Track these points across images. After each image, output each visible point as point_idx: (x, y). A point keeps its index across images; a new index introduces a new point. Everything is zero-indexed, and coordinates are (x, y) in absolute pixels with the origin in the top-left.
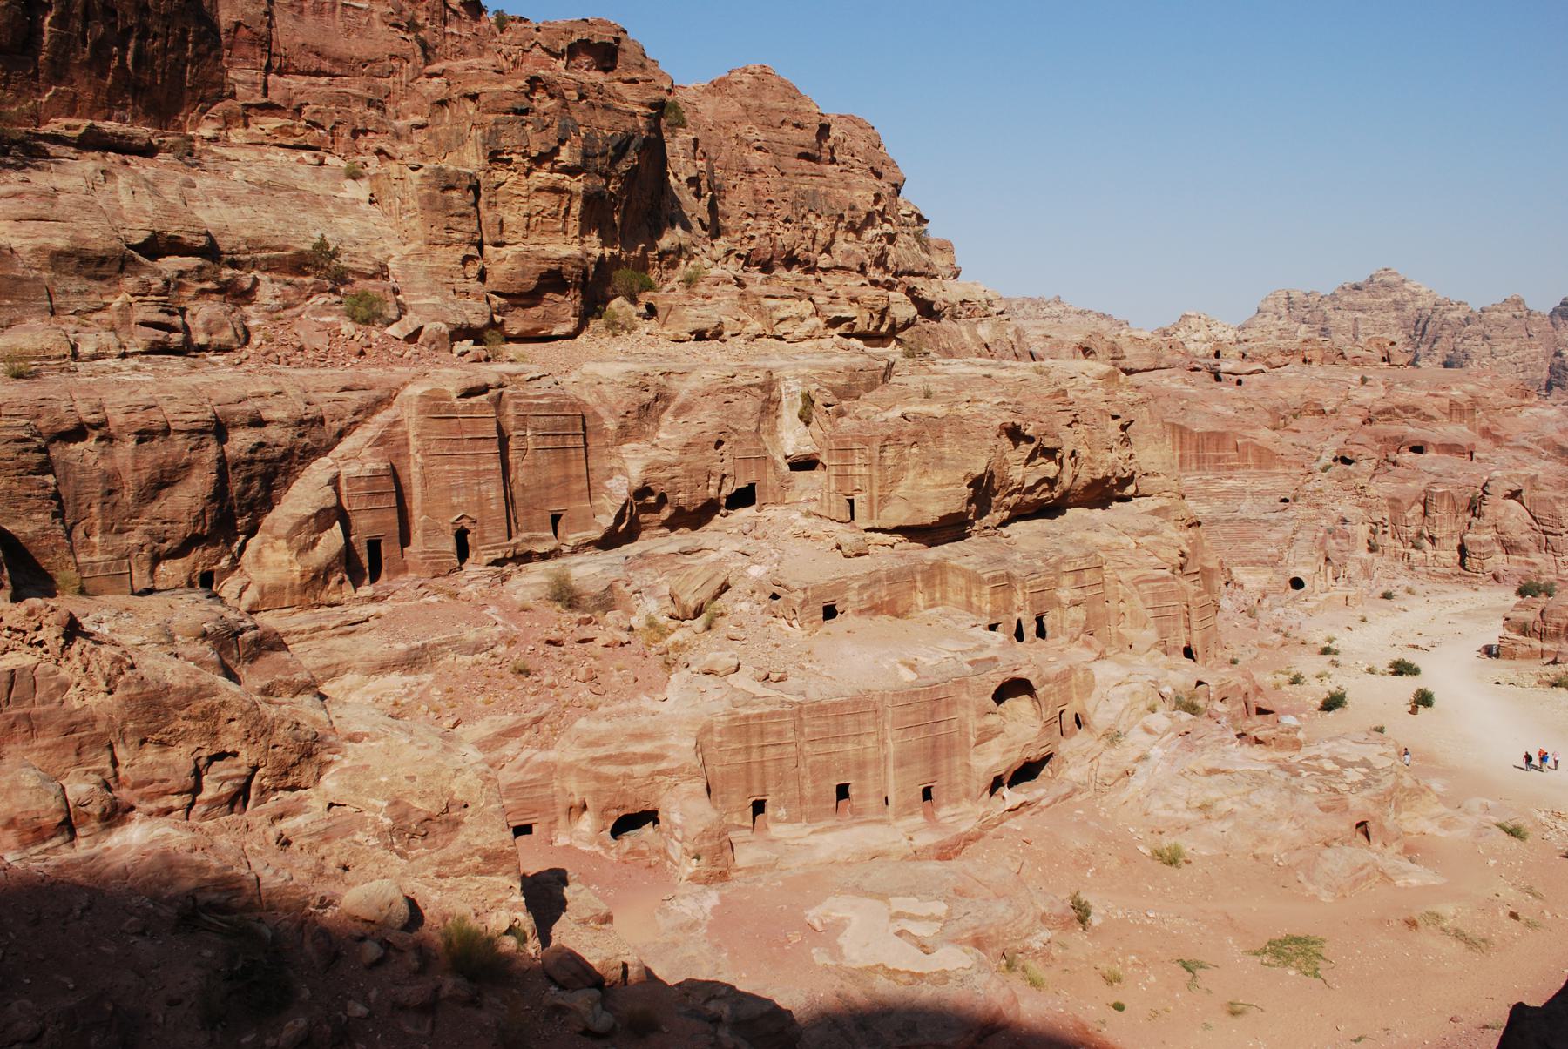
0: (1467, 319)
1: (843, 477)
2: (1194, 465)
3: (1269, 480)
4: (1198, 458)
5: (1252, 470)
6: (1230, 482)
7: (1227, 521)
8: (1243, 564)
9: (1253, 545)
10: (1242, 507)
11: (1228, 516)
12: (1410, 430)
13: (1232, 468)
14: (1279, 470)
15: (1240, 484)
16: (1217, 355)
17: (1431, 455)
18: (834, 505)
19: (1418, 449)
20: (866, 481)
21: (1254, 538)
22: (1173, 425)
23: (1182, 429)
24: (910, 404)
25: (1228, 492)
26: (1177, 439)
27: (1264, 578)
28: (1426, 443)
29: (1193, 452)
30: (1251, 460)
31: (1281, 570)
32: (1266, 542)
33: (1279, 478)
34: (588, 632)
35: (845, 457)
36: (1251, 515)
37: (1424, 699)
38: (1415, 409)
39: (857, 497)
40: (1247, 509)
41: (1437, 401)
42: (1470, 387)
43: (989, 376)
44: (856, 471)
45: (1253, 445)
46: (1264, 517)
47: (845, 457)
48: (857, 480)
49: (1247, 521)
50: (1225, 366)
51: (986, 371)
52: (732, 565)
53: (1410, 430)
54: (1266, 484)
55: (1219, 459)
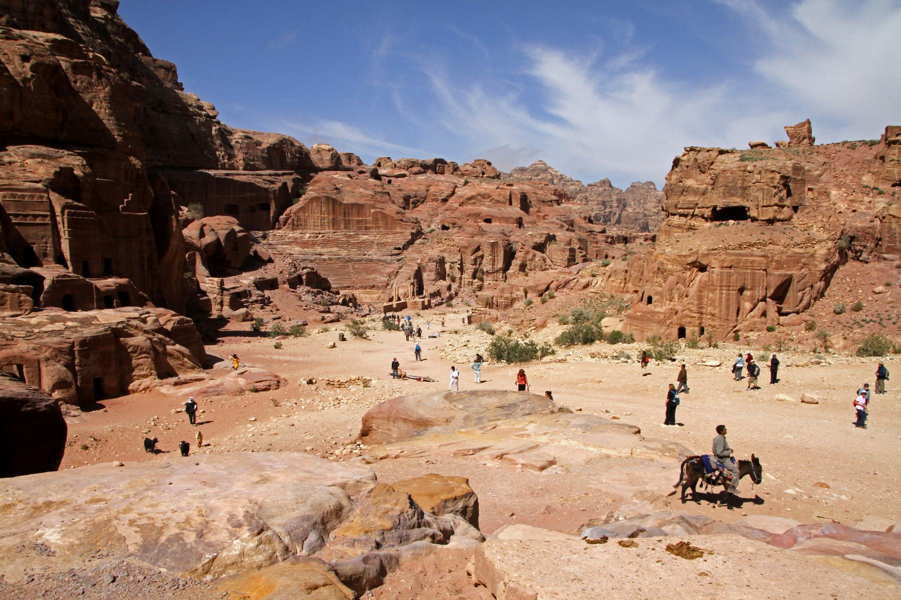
2: (342, 226)
7: (358, 261)
8: (362, 287)
9: (372, 276)
11: (360, 257)
13: (366, 228)
15: (372, 238)
19: (488, 221)
21: (374, 271)
22: (327, 198)
23: (334, 201)
25: (363, 242)
26: (331, 207)
27: (376, 296)
28: (493, 216)
29: (341, 217)
30: (381, 223)
32: (381, 274)
33: (397, 235)
36: (375, 257)
40: (373, 253)
46: (383, 258)
49: (371, 260)
54: (390, 239)
55: (359, 222)
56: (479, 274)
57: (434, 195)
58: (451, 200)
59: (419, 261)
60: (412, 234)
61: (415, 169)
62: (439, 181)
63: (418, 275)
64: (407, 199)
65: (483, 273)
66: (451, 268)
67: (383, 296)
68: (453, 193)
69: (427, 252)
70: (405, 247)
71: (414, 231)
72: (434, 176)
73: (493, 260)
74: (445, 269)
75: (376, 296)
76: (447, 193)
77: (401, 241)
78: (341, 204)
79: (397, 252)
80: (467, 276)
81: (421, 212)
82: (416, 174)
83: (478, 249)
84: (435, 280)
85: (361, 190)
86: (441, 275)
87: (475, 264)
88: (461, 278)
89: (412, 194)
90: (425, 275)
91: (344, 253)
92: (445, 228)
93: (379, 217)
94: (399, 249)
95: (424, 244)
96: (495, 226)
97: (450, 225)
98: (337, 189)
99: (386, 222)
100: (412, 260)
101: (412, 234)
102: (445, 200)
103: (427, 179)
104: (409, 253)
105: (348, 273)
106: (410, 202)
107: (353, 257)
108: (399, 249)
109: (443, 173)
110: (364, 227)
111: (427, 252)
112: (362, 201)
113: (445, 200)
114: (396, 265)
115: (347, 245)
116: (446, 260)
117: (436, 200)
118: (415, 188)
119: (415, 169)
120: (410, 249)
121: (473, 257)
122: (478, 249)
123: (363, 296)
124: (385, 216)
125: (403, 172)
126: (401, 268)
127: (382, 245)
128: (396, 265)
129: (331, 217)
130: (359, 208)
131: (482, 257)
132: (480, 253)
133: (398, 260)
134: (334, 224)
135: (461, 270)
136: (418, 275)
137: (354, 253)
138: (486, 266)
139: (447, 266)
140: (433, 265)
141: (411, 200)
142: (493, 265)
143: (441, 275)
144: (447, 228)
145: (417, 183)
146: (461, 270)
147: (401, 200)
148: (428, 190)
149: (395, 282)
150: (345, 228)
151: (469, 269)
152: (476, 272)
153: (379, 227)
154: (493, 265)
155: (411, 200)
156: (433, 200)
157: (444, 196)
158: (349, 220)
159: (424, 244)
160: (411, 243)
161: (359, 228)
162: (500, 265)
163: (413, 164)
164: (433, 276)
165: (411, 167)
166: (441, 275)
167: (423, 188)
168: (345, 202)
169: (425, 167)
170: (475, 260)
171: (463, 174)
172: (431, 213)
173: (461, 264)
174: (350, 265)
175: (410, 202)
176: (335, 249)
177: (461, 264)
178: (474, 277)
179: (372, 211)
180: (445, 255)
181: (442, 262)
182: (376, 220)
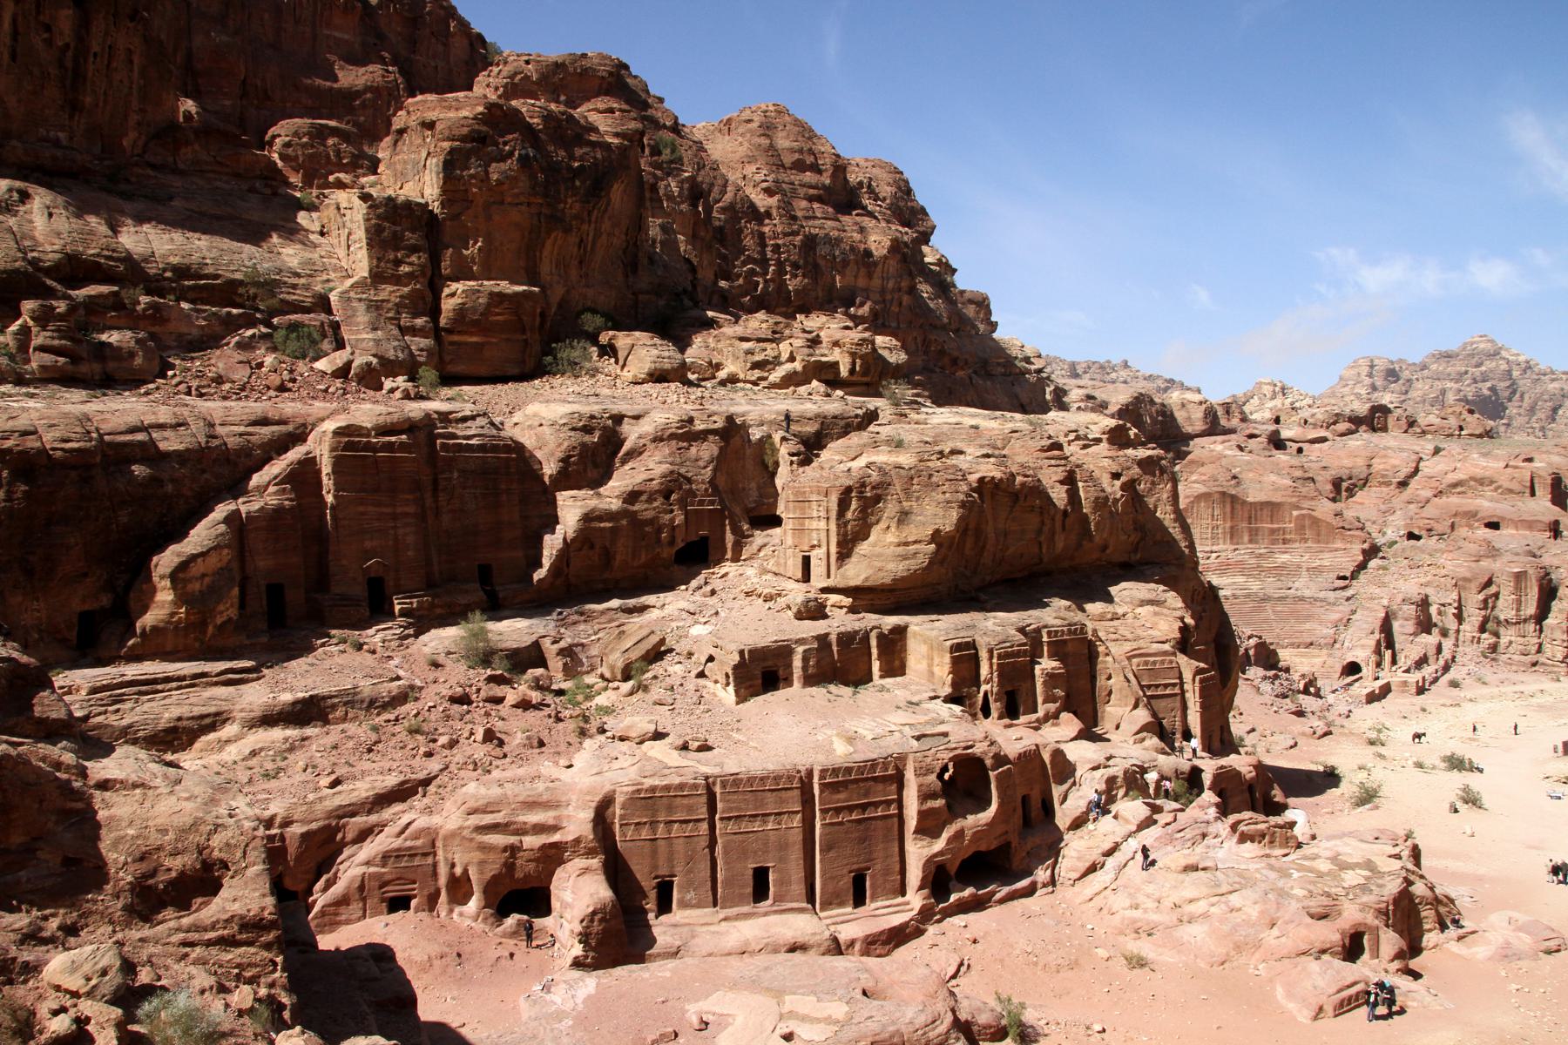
1: (800, 531)
2: (1246, 538)
3: (1327, 555)
4: (1250, 530)
5: (1309, 544)
6: (1285, 557)
8: (1292, 645)
9: (1307, 626)
10: (1297, 584)
12: (1486, 504)
13: (1285, 542)
14: (1339, 545)
15: (1297, 559)
16: (1277, 420)
17: (1506, 532)
18: (790, 562)
19: (1494, 526)
20: (823, 535)
21: (1309, 618)
22: (1223, 494)
23: (1234, 499)
24: (878, 453)
25: (1283, 567)
26: (1228, 509)
27: (1318, 661)
29: (1245, 525)
31: (1338, 653)
32: (1321, 622)
34: (498, 691)
35: (803, 509)
36: (1307, 593)
37: (1471, 799)
38: (1492, 482)
39: (813, 554)
40: (1303, 586)
41: (1516, 473)
42: (1556, 459)
43: (976, 427)
44: (815, 524)
45: (1311, 517)
46: (1322, 595)
47: (803, 509)
48: (814, 535)
49: (1302, 599)
50: (1285, 434)
51: (973, 422)
52: (674, 625)
53: (1486, 504)
54: (1326, 560)
55: (1273, 531)
56: (1490, 626)
57: (1383, 476)
58: (1414, 483)
59: (1385, 602)
60: (1364, 551)
61: (1343, 426)
62: (1386, 448)
63: (1386, 627)
64: (1337, 484)
65: (1499, 623)
66: (1440, 613)
67: (1330, 661)
68: (1417, 470)
69: (1393, 585)
70: (1354, 575)
71: (1366, 546)
72: (1376, 438)
73: (1519, 602)
74: (1429, 617)
75: (1318, 661)
76: (1405, 471)
77: (1347, 565)
78: (1244, 502)
79: (1341, 583)
80: (1470, 627)
81: (1364, 505)
82: (1342, 435)
83: (1489, 583)
84: (1415, 634)
85: (1273, 478)
86: (1425, 625)
87: (1485, 608)
88: (1458, 631)
89: (1344, 473)
90: (1396, 625)
91: (1255, 586)
92: (1411, 536)
93: (1307, 522)
94: (1344, 578)
95: (1385, 568)
96: (1507, 537)
97: (1423, 533)
98: (1235, 477)
99: (1312, 529)
100: (1372, 599)
101: (1364, 551)
102: (1403, 484)
103: (1366, 447)
104: (1361, 585)
105: (1266, 621)
106: (1342, 488)
107: (1270, 592)
108: (1344, 578)
109: (1384, 429)
110: (1280, 538)
111: (1393, 585)
112: (1277, 498)
113: (1403, 484)
114: (1346, 608)
115: (1258, 571)
116: (1431, 599)
117: (1388, 484)
118: (1347, 462)
119: (1343, 426)
120: (1362, 577)
121: (1481, 597)
122: (1489, 583)
123: (1297, 660)
124: (1315, 522)
125: (1322, 433)
126: (1354, 612)
127: (1315, 571)
128: (1346, 608)
129: (1228, 525)
130: (1272, 508)
131: (1496, 595)
132: (1493, 589)
133: (1348, 599)
134: (1233, 534)
135: (1459, 617)
136: (1386, 627)
137: (1271, 586)
138: (1505, 610)
139: (1433, 610)
140: (1411, 610)
141: (1345, 485)
142: (1518, 610)
143: (1425, 625)
144: (1418, 538)
145: (1349, 453)
146: (1459, 617)
147: (1329, 487)
148: (1369, 466)
149: (1348, 637)
150: (1251, 541)
151: (1474, 617)
152: (1486, 620)
153: (1306, 540)
154: (1518, 610)
155: (1345, 485)
156: (1381, 484)
157: (1401, 477)
158: (1257, 529)
159: (1385, 568)
160: (1362, 566)
161: (1274, 542)
162: (1531, 609)
163: (1337, 418)
164: (1410, 627)
165: (1335, 423)
166: (1425, 625)
167: (1361, 462)
168: (1250, 499)
169: (1357, 422)
170: (1485, 601)
171: (1424, 432)
172: (1383, 507)
173: (1459, 608)
174: (1268, 606)
175: (1342, 488)
176: (1240, 579)
177: (1459, 608)
178: (1482, 629)
179: (1295, 513)
180: (1429, 591)
181: (1424, 603)
182: (1300, 529)
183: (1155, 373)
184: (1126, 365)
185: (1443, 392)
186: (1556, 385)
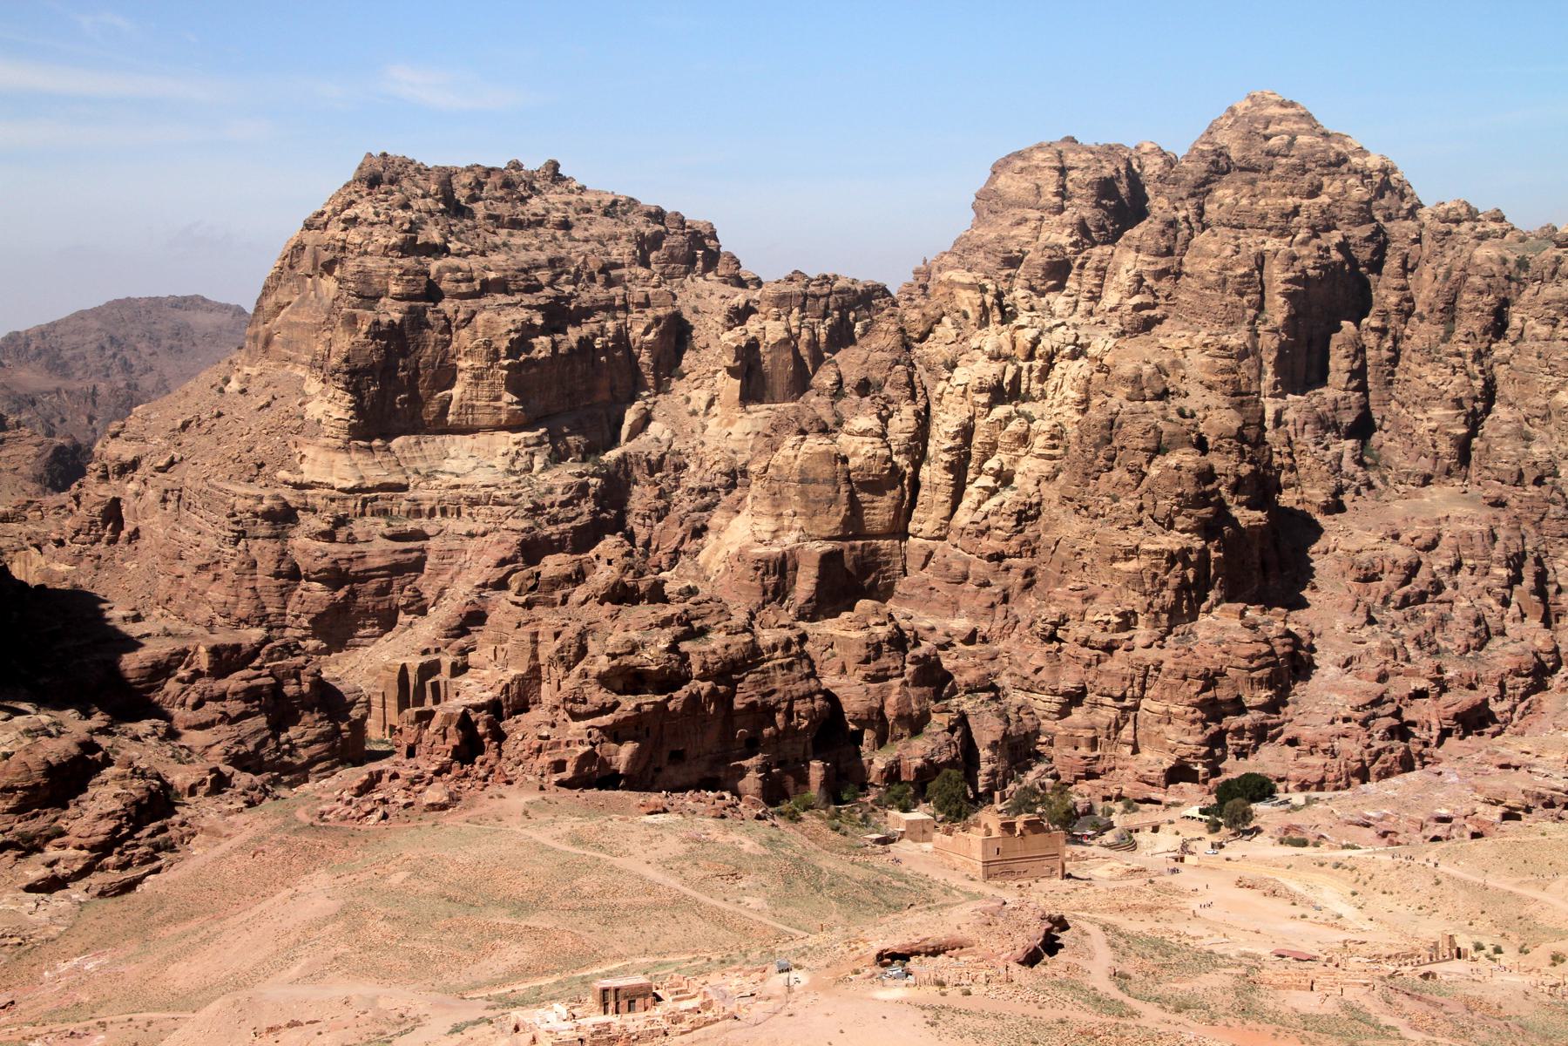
0: (1523, 264)
183: (623, 192)
184: (554, 174)
185: (1260, 261)
186: (1484, 252)
